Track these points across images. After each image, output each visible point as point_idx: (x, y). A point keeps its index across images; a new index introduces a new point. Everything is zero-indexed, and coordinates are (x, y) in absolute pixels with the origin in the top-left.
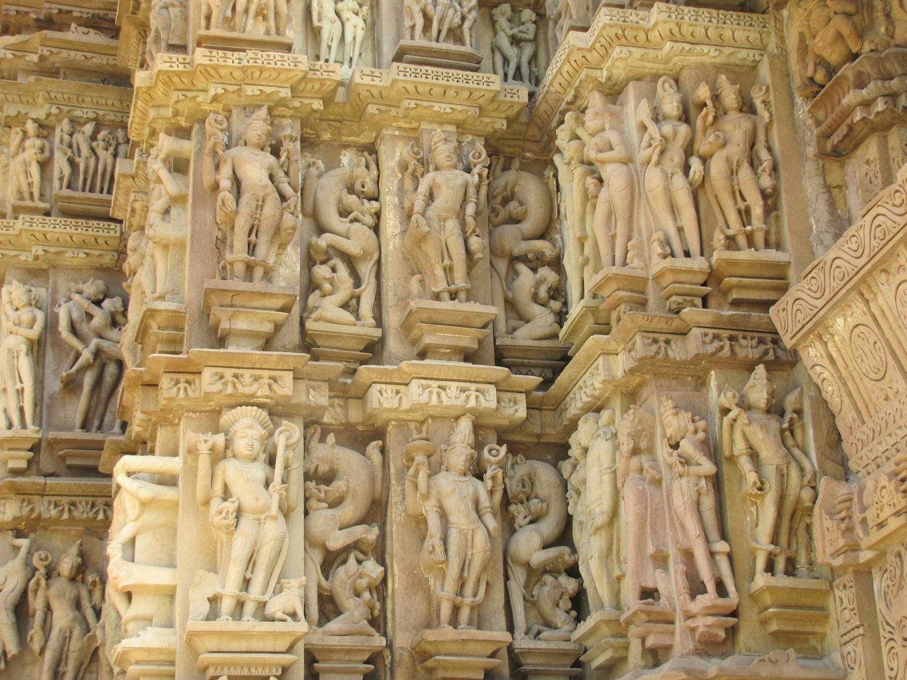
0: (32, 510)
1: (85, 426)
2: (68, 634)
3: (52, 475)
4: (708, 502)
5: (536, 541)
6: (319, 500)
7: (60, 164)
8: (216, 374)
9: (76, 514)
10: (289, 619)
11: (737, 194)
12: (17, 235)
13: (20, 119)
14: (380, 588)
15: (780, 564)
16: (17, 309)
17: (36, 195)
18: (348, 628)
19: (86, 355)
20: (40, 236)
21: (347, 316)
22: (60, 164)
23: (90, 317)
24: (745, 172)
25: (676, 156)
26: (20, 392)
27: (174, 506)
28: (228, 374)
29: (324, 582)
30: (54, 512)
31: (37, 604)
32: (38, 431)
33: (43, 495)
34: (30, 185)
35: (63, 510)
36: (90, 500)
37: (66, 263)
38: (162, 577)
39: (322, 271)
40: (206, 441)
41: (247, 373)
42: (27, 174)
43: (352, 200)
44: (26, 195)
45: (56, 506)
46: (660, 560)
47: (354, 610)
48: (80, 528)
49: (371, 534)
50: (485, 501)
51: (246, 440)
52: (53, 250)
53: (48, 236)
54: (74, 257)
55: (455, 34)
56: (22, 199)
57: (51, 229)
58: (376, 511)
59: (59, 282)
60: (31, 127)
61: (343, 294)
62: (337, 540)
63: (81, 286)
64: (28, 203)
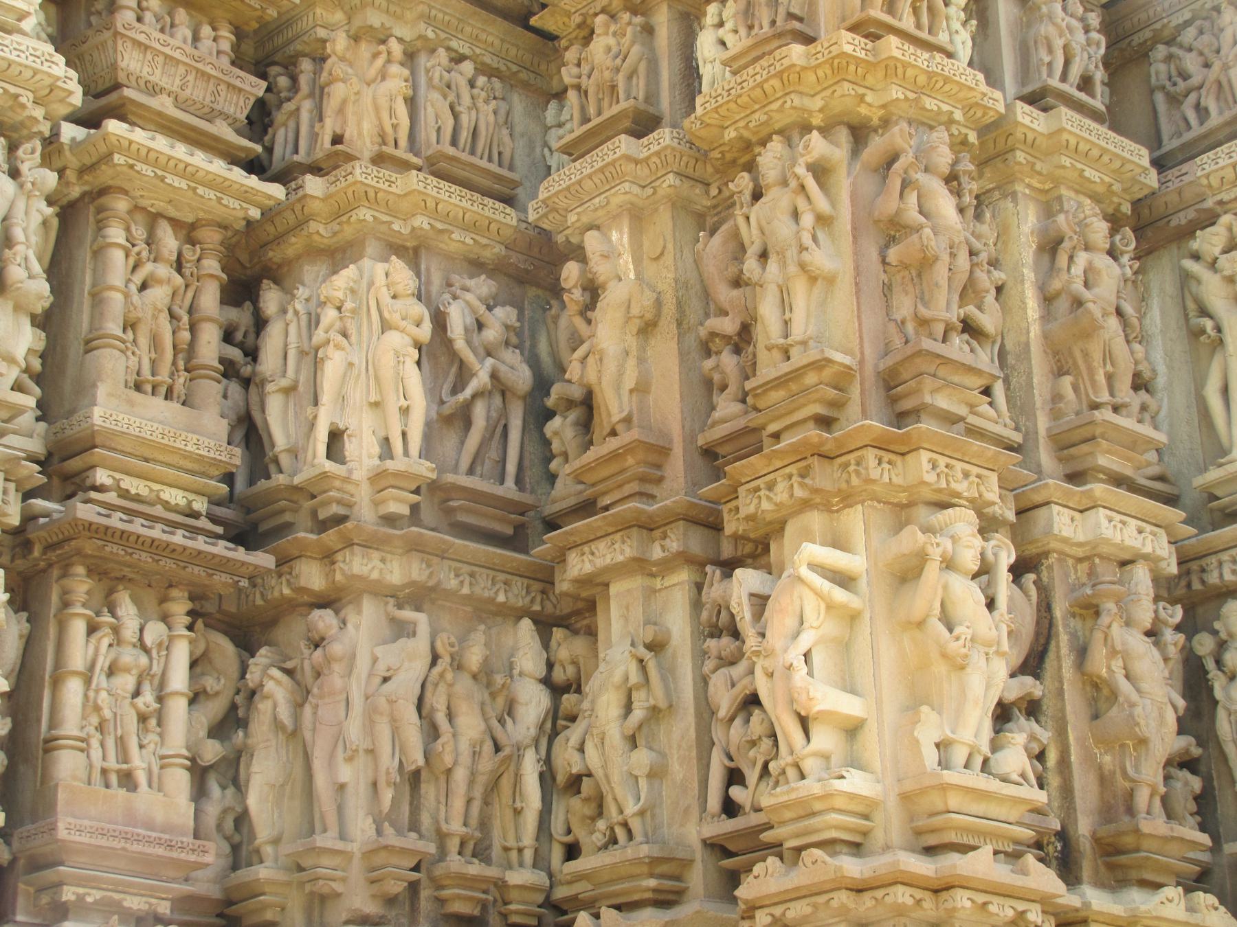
0: (431, 574)
1: (471, 471)
2: (478, 749)
3: (433, 530)
7: (434, 107)
9: (478, 590)
12: (399, 196)
16: (394, 297)
19: (481, 379)
20: (431, 204)
22: (434, 107)
23: (480, 326)
26: (405, 411)
27: (853, 618)
28: (942, 461)
30: (453, 583)
31: (437, 701)
32: (433, 470)
33: (443, 558)
34: (395, 127)
35: (462, 582)
36: (492, 573)
37: (441, 245)
38: (851, 706)
41: (959, 466)
42: (392, 113)
45: (457, 576)
48: (469, 609)
52: (439, 226)
53: (440, 207)
54: (460, 241)
56: (384, 143)
57: (446, 198)
59: (432, 270)
60: (396, 48)
63: (471, 283)
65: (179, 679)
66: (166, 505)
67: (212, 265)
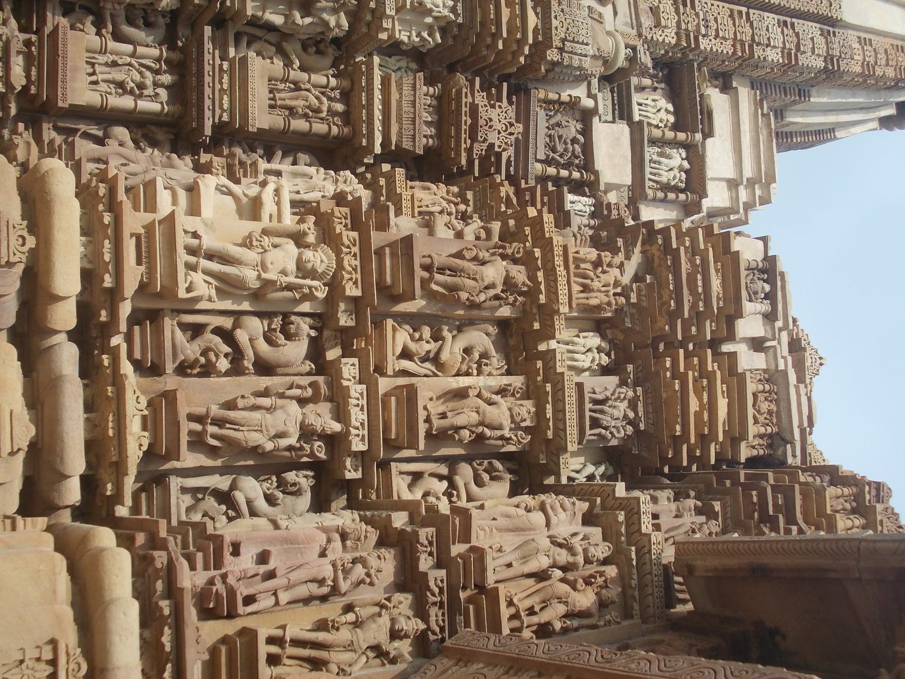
4: (314, 589)
5: (252, 495)
6: (269, 325)
8: (355, 240)
10: (187, 285)
11: (545, 604)
13: (466, 202)
14: (208, 370)
15: (274, 649)
17: (421, 209)
18: (178, 342)
21: (399, 351)
24: (562, 609)
25: (563, 557)
28: (356, 249)
29: (210, 328)
39: (426, 332)
40: (309, 229)
43: (476, 356)
44: (420, 204)
46: (263, 558)
47: (191, 350)
49: (248, 364)
50: (284, 442)
51: (312, 259)
55: (595, 423)
58: (264, 368)
61: (413, 346)
62: (242, 336)
64: (416, 204)
65: (145, 105)
66: (221, 99)
67: (335, 130)
